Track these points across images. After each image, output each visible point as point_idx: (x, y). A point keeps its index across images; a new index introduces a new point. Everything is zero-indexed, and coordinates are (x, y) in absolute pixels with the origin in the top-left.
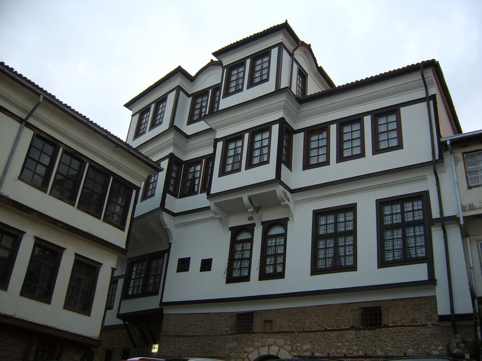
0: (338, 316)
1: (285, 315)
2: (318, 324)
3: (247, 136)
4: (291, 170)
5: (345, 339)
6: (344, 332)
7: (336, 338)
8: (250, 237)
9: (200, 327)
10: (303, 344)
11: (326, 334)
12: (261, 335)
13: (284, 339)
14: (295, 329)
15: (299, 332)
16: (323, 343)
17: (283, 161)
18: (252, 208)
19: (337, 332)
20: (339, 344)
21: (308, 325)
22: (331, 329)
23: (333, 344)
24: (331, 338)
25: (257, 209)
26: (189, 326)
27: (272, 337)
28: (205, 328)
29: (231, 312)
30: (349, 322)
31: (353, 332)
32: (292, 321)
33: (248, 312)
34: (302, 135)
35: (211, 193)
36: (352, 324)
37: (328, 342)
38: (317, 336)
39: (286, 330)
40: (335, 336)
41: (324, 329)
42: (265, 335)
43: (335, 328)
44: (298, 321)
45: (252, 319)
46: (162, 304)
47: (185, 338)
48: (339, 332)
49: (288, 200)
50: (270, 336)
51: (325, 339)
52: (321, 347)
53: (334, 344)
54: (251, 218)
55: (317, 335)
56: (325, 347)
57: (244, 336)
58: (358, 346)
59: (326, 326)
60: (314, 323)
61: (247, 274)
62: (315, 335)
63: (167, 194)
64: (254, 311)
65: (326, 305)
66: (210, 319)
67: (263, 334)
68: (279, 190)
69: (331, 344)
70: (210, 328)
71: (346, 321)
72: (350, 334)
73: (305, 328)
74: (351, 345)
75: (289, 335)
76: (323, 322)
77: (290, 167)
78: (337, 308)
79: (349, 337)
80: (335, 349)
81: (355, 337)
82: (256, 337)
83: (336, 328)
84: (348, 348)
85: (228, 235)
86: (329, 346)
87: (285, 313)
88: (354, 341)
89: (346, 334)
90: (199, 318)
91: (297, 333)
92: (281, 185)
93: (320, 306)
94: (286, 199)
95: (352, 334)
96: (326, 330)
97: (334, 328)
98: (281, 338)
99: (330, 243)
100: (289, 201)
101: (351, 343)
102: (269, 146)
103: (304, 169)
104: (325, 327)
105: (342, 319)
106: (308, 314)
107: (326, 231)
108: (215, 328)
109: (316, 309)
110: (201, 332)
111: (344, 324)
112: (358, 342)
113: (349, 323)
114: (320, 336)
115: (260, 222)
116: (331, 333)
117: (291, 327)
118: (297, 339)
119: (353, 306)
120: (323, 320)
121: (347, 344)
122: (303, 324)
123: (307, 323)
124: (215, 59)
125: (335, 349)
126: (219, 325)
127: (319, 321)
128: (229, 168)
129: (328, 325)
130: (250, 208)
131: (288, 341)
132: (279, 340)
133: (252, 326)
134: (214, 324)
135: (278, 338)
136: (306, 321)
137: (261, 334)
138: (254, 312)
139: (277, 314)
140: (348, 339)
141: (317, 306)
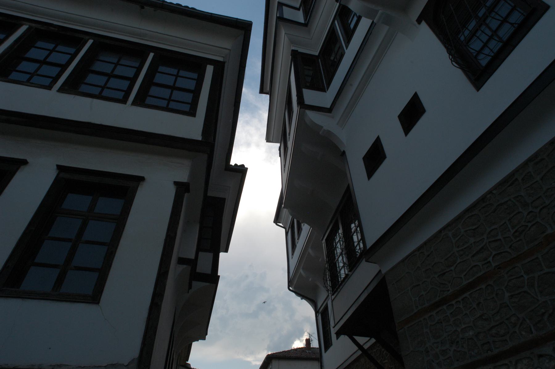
47: (453, 302)
70: (512, 231)
108: (529, 222)
110: (490, 259)
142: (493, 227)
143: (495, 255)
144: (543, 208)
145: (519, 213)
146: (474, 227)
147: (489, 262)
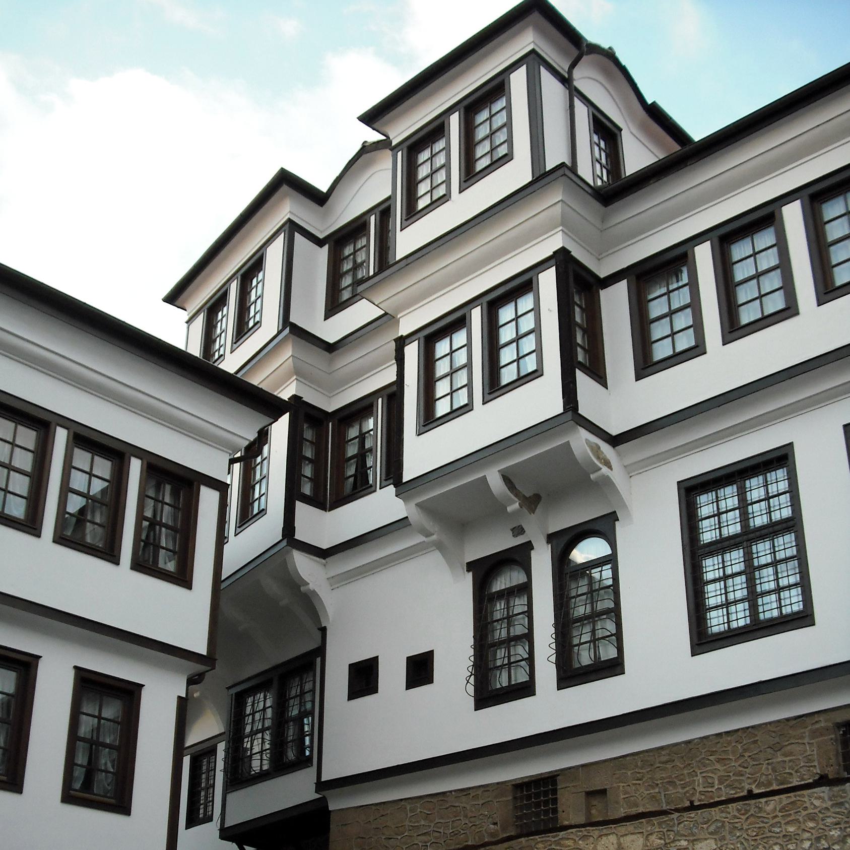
0: (779, 753)
1: (637, 770)
2: (728, 782)
3: (476, 315)
4: (605, 385)
5: (804, 813)
6: (799, 796)
7: (781, 814)
8: (522, 578)
9: (426, 831)
10: (695, 840)
11: (753, 806)
12: (581, 831)
13: (643, 832)
14: (668, 803)
15: (677, 810)
16: (747, 830)
17: (580, 363)
18: (515, 502)
19: (782, 796)
20: (791, 829)
21: (701, 790)
22: (763, 791)
23: (773, 829)
24: (768, 814)
25: (532, 502)
26: (397, 834)
27: (610, 834)
28: (438, 834)
29: (498, 783)
30: (811, 766)
31: (823, 792)
32: (657, 784)
33: (542, 776)
34: (621, 289)
35: (404, 480)
36: (819, 772)
37: (760, 828)
38: (728, 816)
39: (644, 811)
40: (778, 809)
41: (745, 793)
42: (593, 830)
43: (775, 787)
44: (675, 782)
45: (555, 791)
46: (321, 786)
48: (786, 795)
49: (608, 464)
50: (605, 831)
51: (752, 819)
52: (742, 843)
53: (778, 830)
54: (518, 531)
55: (730, 813)
56: (753, 840)
57: (539, 840)
58: (842, 826)
59: (749, 784)
60: (717, 782)
61: (526, 678)
62: (722, 812)
63: (297, 502)
64: (556, 771)
65: (742, 729)
66: (447, 808)
67: (588, 828)
68: (581, 440)
69: (770, 831)
71: (802, 764)
72: (816, 798)
73: (693, 799)
74: (822, 827)
75: (655, 820)
76: (742, 775)
77: (601, 378)
78: (772, 732)
79: (815, 807)
80: (780, 845)
81: (830, 803)
82: (568, 839)
83: (778, 788)
84: (814, 836)
85: (466, 584)
86: (762, 838)
87: (637, 766)
88: (829, 814)
89: (806, 799)
90: (419, 810)
91: (677, 814)
92: (580, 426)
93: (728, 733)
94: (601, 463)
95: (820, 798)
96: (751, 796)
97: (771, 788)
98: (637, 831)
99: (735, 558)
100: (610, 467)
101: (823, 820)
102: (537, 330)
103: (638, 378)
104: (747, 787)
105: (790, 761)
106: (698, 759)
107: (720, 532)
108: (463, 830)
109: (719, 742)
110: (429, 844)
111: (796, 772)
112: (840, 816)
113: (811, 769)
114: (738, 815)
115: (542, 537)
116: (766, 802)
117: (657, 800)
118: (675, 828)
119: (817, 722)
120: (741, 769)
121: (811, 824)
122: (687, 789)
123: (698, 785)
124: (372, 136)
125: (780, 845)
126: (472, 819)
127: (731, 774)
128: (442, 408)
129: (756, 781)
130: (512, 502)
131: (653, 838)
132: (630, 838)
133: (555, 811)
134: (460, 820)
135: (626, 835)
136: (695, 778)
137: (583, 829)
138: (558, 775)
139: (618, 772)
140: (812, 811)
141: (719, 735)
142: (440, 821)
143: (433, 842)
144: (474, 825)
145: (460, 820)
146: (429, 813)
147: (427, 846)
